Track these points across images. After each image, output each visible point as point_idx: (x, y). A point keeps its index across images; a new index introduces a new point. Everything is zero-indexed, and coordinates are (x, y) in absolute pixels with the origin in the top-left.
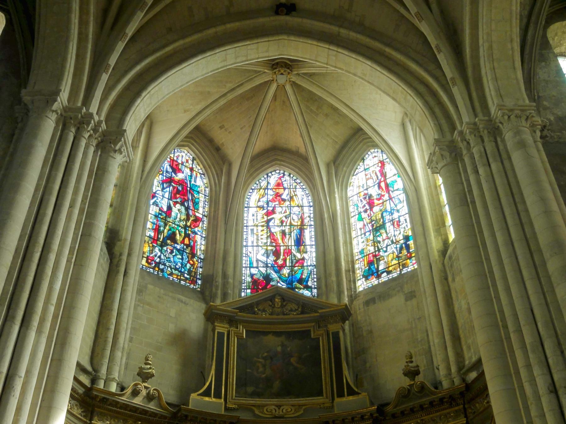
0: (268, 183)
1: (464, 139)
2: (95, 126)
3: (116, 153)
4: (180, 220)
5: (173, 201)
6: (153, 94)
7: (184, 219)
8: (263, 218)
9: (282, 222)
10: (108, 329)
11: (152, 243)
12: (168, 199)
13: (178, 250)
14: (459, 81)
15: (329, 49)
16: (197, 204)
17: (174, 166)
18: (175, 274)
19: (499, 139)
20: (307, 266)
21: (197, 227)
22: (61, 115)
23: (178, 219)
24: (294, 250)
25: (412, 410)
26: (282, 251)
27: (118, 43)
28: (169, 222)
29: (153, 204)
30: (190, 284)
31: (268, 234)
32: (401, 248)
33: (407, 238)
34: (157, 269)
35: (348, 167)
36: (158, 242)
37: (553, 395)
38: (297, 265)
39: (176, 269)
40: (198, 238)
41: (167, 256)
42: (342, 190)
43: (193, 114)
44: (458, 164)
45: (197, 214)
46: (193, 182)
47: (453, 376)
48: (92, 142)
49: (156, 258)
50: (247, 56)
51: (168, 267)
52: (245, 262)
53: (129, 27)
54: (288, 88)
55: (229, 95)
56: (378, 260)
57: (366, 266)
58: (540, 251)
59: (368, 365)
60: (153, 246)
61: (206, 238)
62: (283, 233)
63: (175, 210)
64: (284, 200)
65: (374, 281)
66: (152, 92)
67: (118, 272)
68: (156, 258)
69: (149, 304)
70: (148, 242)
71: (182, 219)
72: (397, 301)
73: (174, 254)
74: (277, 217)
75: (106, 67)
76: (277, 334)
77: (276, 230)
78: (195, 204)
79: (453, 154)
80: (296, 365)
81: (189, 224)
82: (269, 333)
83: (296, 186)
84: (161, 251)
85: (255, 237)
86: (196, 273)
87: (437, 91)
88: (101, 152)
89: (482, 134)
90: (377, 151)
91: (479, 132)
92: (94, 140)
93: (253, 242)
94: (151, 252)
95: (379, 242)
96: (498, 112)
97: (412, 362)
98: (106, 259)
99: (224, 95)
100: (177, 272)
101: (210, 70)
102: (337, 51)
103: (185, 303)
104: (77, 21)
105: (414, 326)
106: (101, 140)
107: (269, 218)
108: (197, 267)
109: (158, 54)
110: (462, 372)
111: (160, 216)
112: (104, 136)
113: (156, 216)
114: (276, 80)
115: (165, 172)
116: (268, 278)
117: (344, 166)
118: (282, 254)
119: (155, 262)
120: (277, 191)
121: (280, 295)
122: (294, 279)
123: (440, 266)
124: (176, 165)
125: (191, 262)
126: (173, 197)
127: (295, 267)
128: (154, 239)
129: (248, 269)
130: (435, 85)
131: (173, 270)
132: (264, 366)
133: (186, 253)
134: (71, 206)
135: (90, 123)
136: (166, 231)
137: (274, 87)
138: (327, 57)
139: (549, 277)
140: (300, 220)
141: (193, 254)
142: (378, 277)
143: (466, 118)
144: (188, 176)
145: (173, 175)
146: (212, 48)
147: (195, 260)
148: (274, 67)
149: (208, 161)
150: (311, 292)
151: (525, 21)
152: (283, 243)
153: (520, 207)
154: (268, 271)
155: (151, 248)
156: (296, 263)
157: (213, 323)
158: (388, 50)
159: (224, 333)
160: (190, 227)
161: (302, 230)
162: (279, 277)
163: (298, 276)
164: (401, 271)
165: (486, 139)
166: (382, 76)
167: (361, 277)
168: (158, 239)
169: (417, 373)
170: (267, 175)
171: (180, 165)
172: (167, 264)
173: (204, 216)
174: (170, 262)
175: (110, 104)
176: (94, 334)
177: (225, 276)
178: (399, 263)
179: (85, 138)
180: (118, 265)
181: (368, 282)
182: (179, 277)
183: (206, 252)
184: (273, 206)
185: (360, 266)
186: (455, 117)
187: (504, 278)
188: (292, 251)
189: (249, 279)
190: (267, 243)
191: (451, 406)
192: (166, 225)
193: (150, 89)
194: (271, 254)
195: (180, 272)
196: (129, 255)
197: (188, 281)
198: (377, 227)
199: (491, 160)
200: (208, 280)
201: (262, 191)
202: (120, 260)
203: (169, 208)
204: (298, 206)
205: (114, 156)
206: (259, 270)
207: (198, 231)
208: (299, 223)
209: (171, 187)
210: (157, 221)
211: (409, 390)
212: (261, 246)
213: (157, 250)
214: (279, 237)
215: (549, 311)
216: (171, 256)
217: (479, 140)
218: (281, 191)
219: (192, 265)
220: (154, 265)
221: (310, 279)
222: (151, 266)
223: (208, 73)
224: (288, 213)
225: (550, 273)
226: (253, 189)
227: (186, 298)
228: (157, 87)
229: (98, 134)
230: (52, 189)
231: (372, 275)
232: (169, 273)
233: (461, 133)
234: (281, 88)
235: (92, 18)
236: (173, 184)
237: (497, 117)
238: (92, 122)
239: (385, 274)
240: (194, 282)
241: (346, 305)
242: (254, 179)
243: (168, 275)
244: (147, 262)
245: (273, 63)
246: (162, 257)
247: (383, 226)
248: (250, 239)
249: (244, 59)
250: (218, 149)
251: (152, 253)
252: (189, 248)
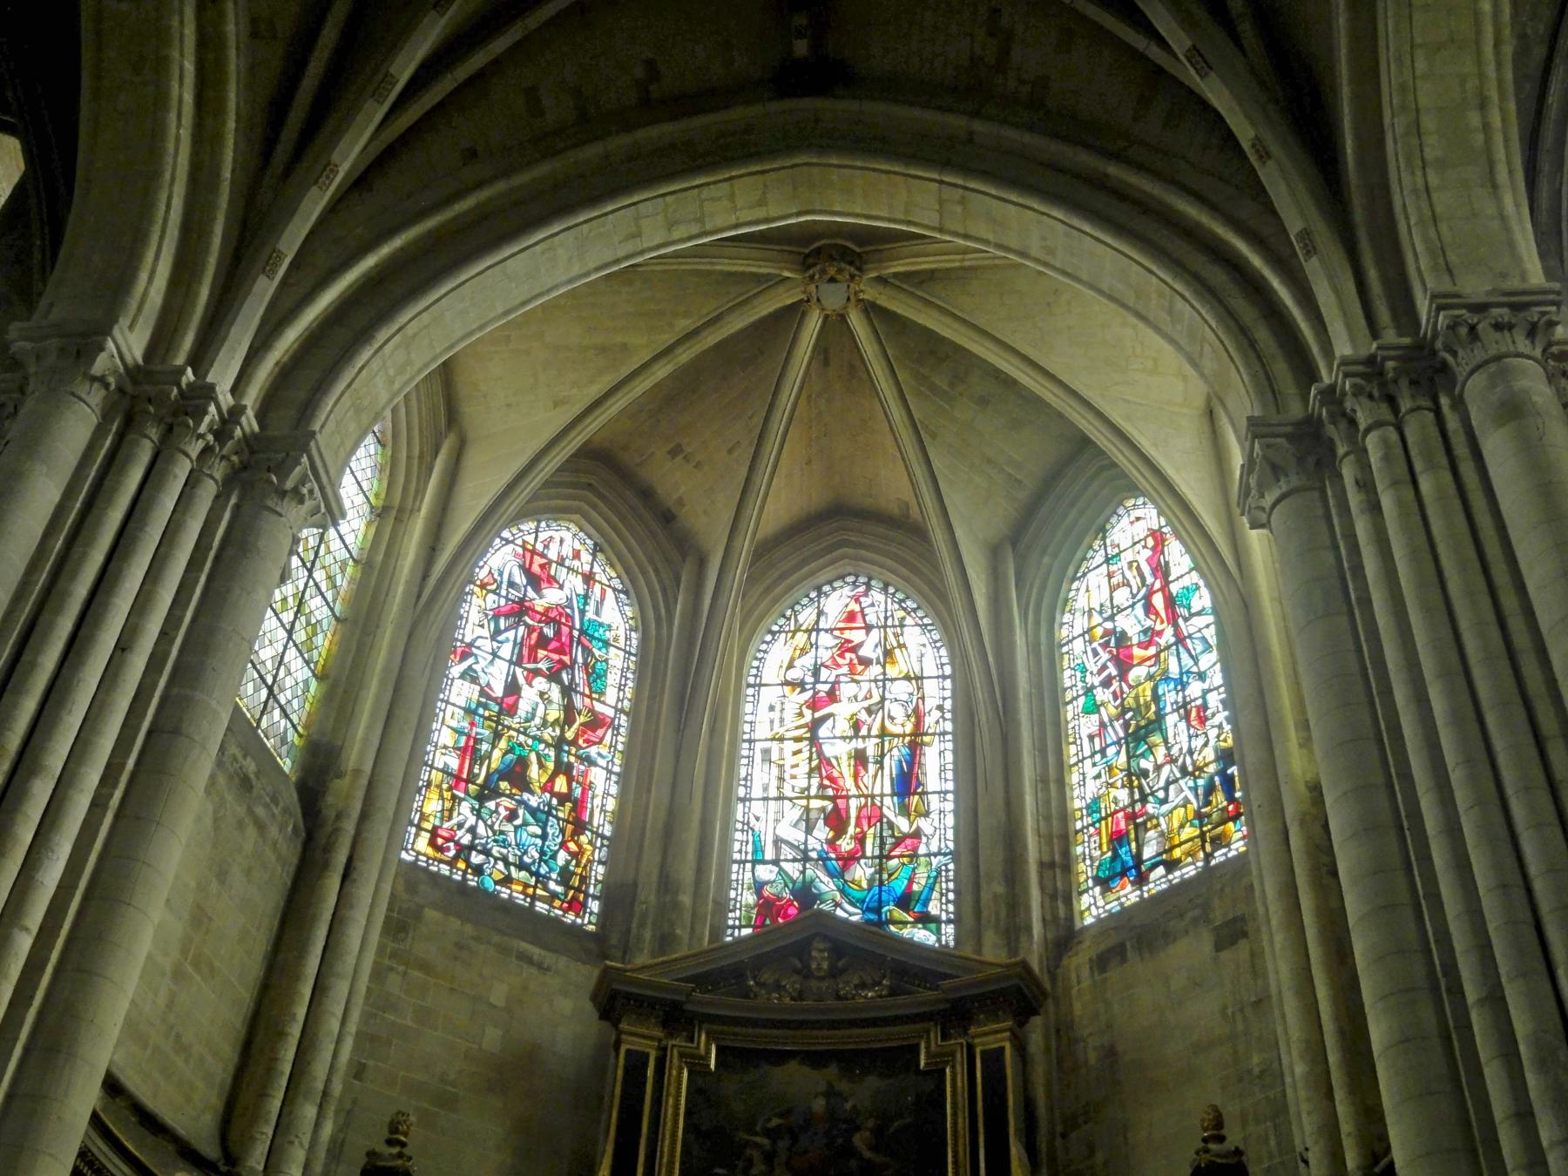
0: (820, 613)
2: (223, 421)
3: (286, 500)
4: (545, 724)
5: (525, 669)
6: (415, 335)
7: (557, 720)
8: (801, 715)
9: (857, 726)
10: (281, 1035)
11: (450, 789)
12: (511, 662)
13: (533, 812)
14: (1324, 236)
15: (941, 182)
16: (599, 677)
17: (536, 569)
18: (519, 882)
19: (1444, 401)
20: (929, 855)
21: (595, 743)
22: (121, 390)
23: (537, 721)
24: (890, 808)
26: (853, 813)
27: (309, 189)
28: (510, 728)
29: (463, 676)
30: (566, 911)
31: (814, 763)
32: (1210, 789)
33: (1225, 757)
34: (462, 865)
35: (1055, 556)
36: (472, 787)
38: (896, 852)
39: (522, 866)
40: (597, 776)
41: (496, 827)
42: (1037, 622)
43: (577, 409)
44: (1323, 491)
45: (598, 707)
46: (590, 615)
48: (210, 468)
49: (459, 833)
50: (701, 220)
51: (496, 859)
52: (740, 845)
53: (342, 145)
54: (856, 321)
55: (680, 350)
56: (1141, 828)
57: (1105, 849)
59: (1100, 1157)
60: (454, 797)
61: (623, 779)
62: (860, 758)
63: (529, 697)
64: (866, 662)
65: (1129, 895)
66: (410, 330)
67: (326, 865)
68: (459, 833)
69: (425, 967)
70: (439, 787)
71: (551, 718)
73: (518, 822)
74: (843, 711)
75: (270, 257)
76: (816, 1059)
77: (839, 750)
78: (595, 675)
80: (867, 1154)
81: (570, 735)
82: (791, 1055)
83: (903, 619)
84: (478, 814)
85: (775, 771)
86: (584, 879)
88: (241, 498)
89: (1391, 389)
90: (1144, 504)
92: (218, 461)
93: (766, 789)
94: (447, 814)
95: (1145, 773)
96: (1437, 316)
98: (290, 829)
99: (668, 351)
100: (523, 875)
101: (592, 265)
102: (966, 188)
103: (540, 966)
104: (186, 134)
105: (1240, 1027)
106: (241, 462)
107: (817, 715)
108: (589, 861)
109: (430, 223)
111: (481, 711)
112: (253, 452)
113: (469, 711)
114: (818, 300)
115: (504, 586)
116: (805, 894)
117: (1044, 552)
118: (853, 821)
119: (457, 844)
120: (847, 635)
121: (825, 938)
122: (885, 897)
124: (542, 566)
125: (572, 846)
126: (524, 655)
127: (889, 858)
128: (458, 778)
129: (748, 866)
131: (512, 868)
132: (769, 1157)
133: (558, 819)
134: (123, 647)
135: (205, 412)
136: (497, 754)
137: (813, 325)
138: (937, 207)
140: (913, 719)
141: (579, 826)
142: (1141, 880)
143: (1343, 348)
144: (578, 595)
145: (531, 593)
146: (593, 199)
147: (583, 839)
148: (811, 261)
149: (640, 553)
150: (938, 932)
151: (1539, 52)
152: (858, 787)
153: (1509, 602)
154: (809, 873)
155: (448, 805)
156: (896, 845)
157: (615, 1025)
158: (1114, 170)
159: (647, 1056)
160: (574, 742)
161: (915, 747)
162: (842, 891)
163: (899, 886)
164: (1208, 857)
166: (1100, 248)
167: (1090, 883)
168: (471, 779)
170: (819, 589)
171: (554, 565)
172: (496, 851)
173: (622, 711)
174: (504, 844)
175: (277, 364)
176: (238, 1049)
177: (667, 884)
178: (1202, 835)
179: (187, 456)
180: (328, 848)
181: (1112, 897)
182: (530, 891)
183: (618, 818)
184: (832, 679)
185: (1090, 851)
187: (1453, 830)
188: (885, 811)
189: (750, 898)
190: (808, 789)
192: (497, 736)
193: (403, 318)
194: (821, 822)
195: (537, 874)
196: (364, 816)
197: (557, 903)
198: (1138, 728)
199: (1418, 466)
200: (618, 897)
201: (801, 638)
202: (336, 831)
203: (513, 688)
204: (907, 678)
205: (278, 509)
206: (781, 871)
207: (599, 754)
208: (909, 728)
209: (521, 629)
210: (472, 724)
212: (790, 799)
213: (465, 808)
214: (846, 769)
216: (509, 827)
218: (856, 636)
219: (576, 856)
220: (452, 853)
221: (935, 895)
222: (443, 857)
223: (587, 274)
224: (876, 698)
226: (773, 633)
227: (543, 952)
228: (425, 315)
229: (230, 444)
230: (66, 595)
231: (1123, 874)
232: (499, 877)
234: (836, 325)
235: (231, 124)
236: (527, 619)
237: (1435, 335)
238: (212, 409)
239: (1161, 870)
240: (577, 906)
241: (1025, 965)
242: (776, 601)
243: (496, 883)
244: (432, 843)
245: (807, 251)
246: (481, 829)
247: (1157, 723)
248: (760, 777)
249: (695, 229)
250: (668, 518)
251: (450, 818)
252: (569, 805)
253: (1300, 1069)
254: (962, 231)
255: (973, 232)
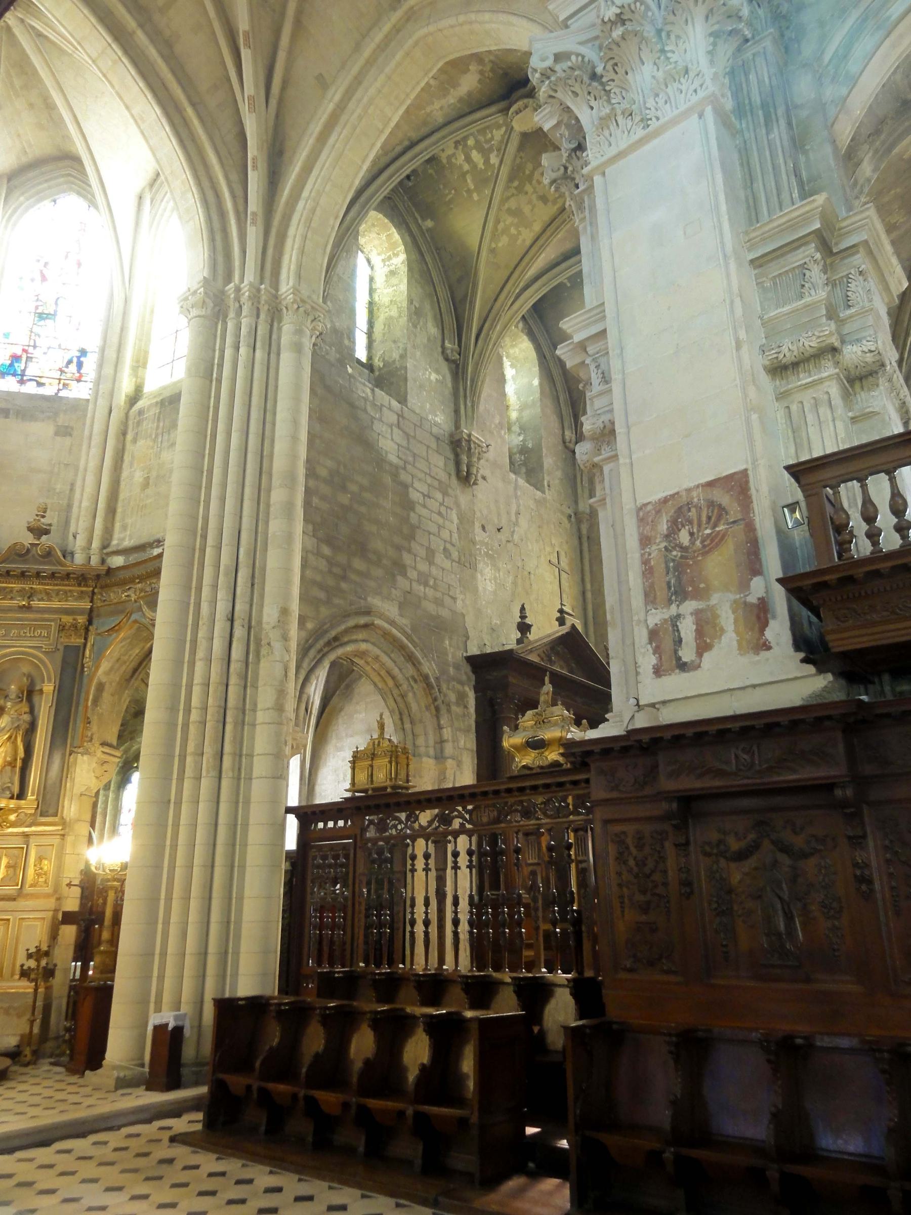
1: (237, 299)
19: (275, 324)
25: (23, 575)
32: (70, 362)
37: (229, 623)
44: (217, 324)
47: (92, 552)
58: (270, 475)
72: (42, 429)
79: (217, 308)
87: (228, 212)
89: (261, 306)
91: (259, 302)
97: (43, 517)
105: (56, 470)
110: (105, 551)
117: (23, 194)
123: (122, 415)
130: (229, 205)
139: (268, 505)
142: (22, 382)
158: (190, 112)
164: (59, 390)
165: (263, 316)
169: (47, 532)
186: (237, 263)
187: (224, 485)
191: (79, 585)
211: (28, 551)
215: (256, 540)
217: (255, 313)
225: (272, 502)
231: (14, 375)
233: (238, 290)
237: (286, 298)
253: (85, 504)
254: (105, 72)
255: (108, 76)
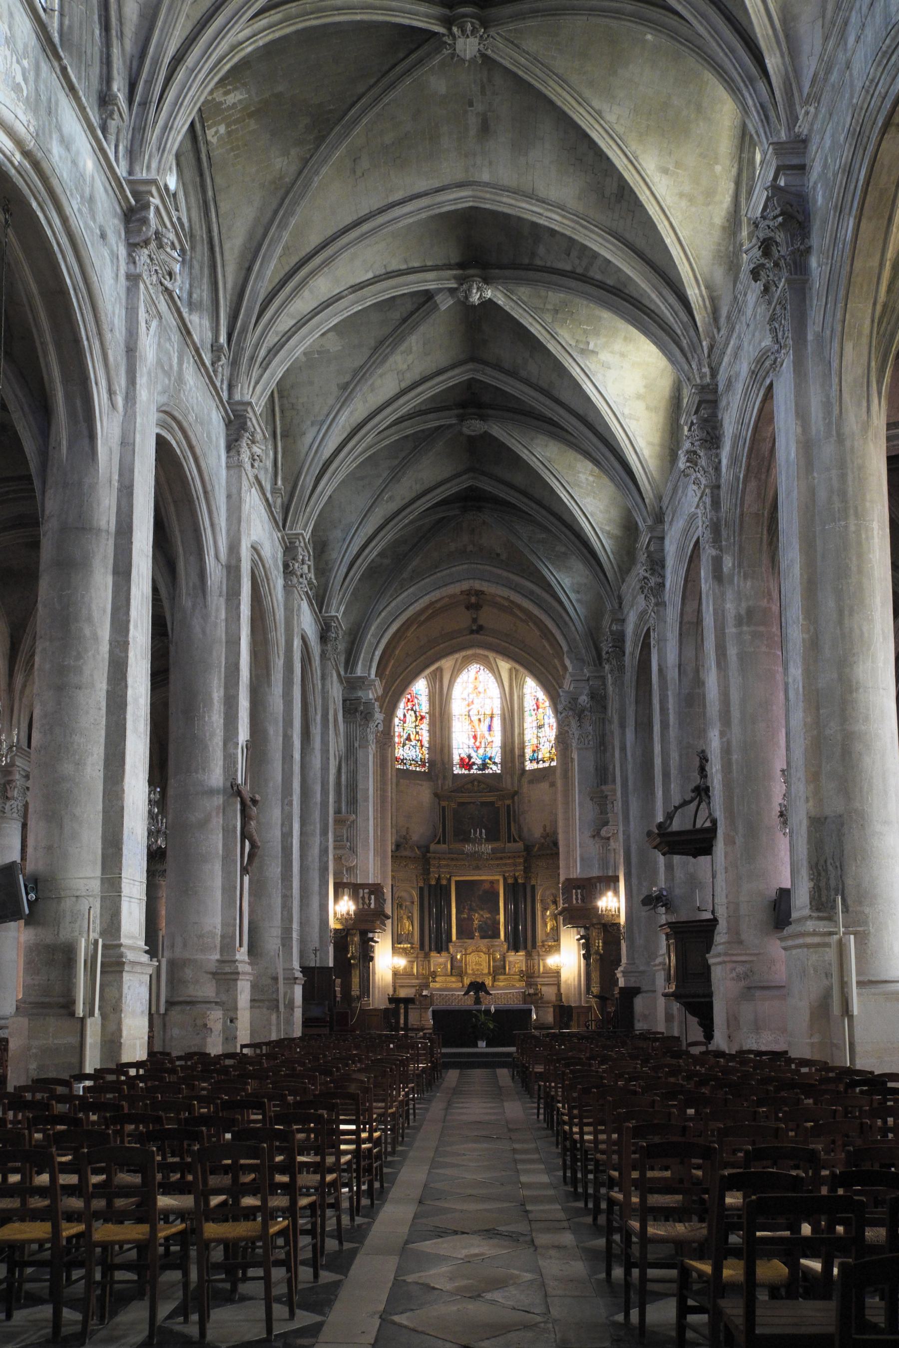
61: (429, 731)
62: (480, 720)
78: (419, 705)
116: (470, 757)
141: (422, 746)
183: (430, 742)
200: (432, 762)
203: (405, 716)
214: (476, 722)
